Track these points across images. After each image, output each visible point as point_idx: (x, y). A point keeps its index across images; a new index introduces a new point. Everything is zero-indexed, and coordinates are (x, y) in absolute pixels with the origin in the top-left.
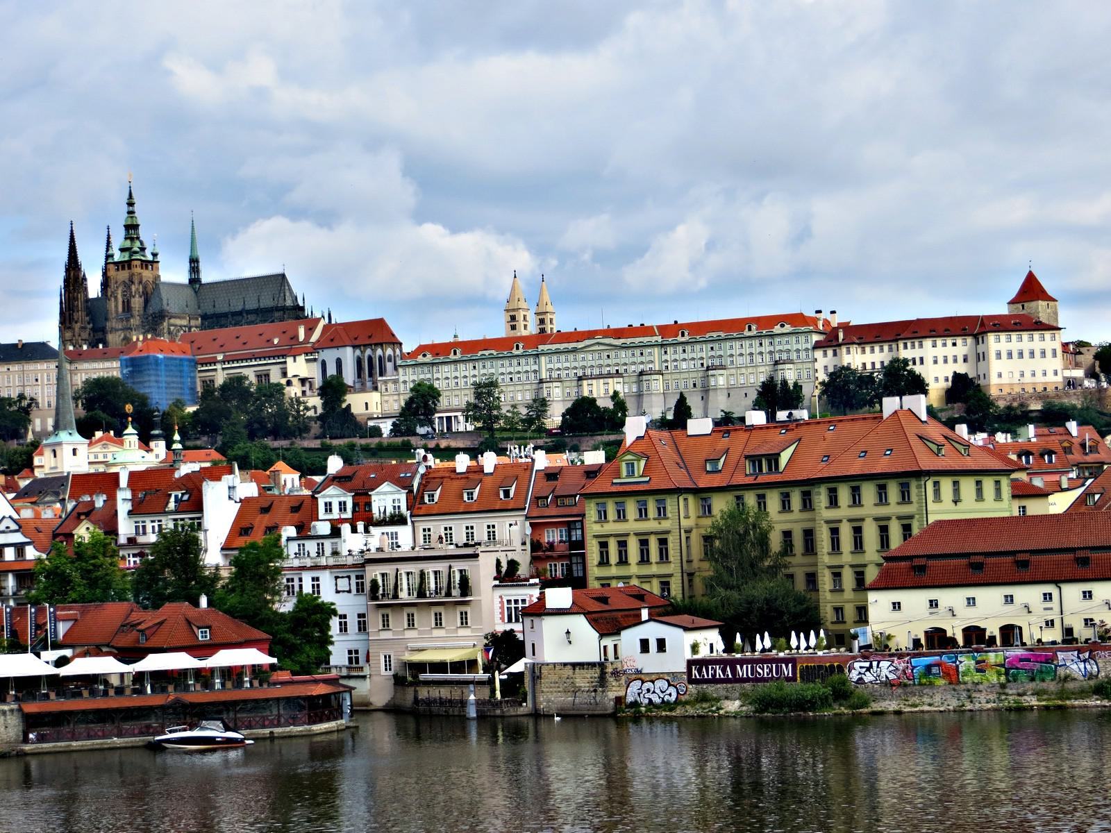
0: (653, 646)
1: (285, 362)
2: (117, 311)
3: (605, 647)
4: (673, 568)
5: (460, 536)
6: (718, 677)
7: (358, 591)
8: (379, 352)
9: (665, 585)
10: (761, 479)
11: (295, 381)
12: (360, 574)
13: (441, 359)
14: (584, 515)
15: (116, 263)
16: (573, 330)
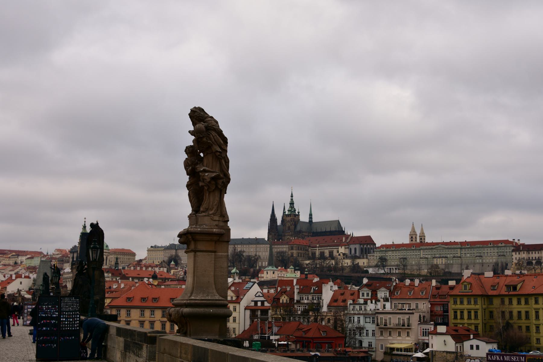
0: (475, 347)
1: (338, 248)
2: (286, 230)
3: (457, 347)
4: (479, 321)
6: (497, 359)
7: (373, 323)
8: (369, 246)
9: (476, 327)
10: (510, 293)
11: (341, 254)
12: (374, 317)
13: (388, 249)
14: (449, 302)
15: (286, 215)
16: (432, 242)
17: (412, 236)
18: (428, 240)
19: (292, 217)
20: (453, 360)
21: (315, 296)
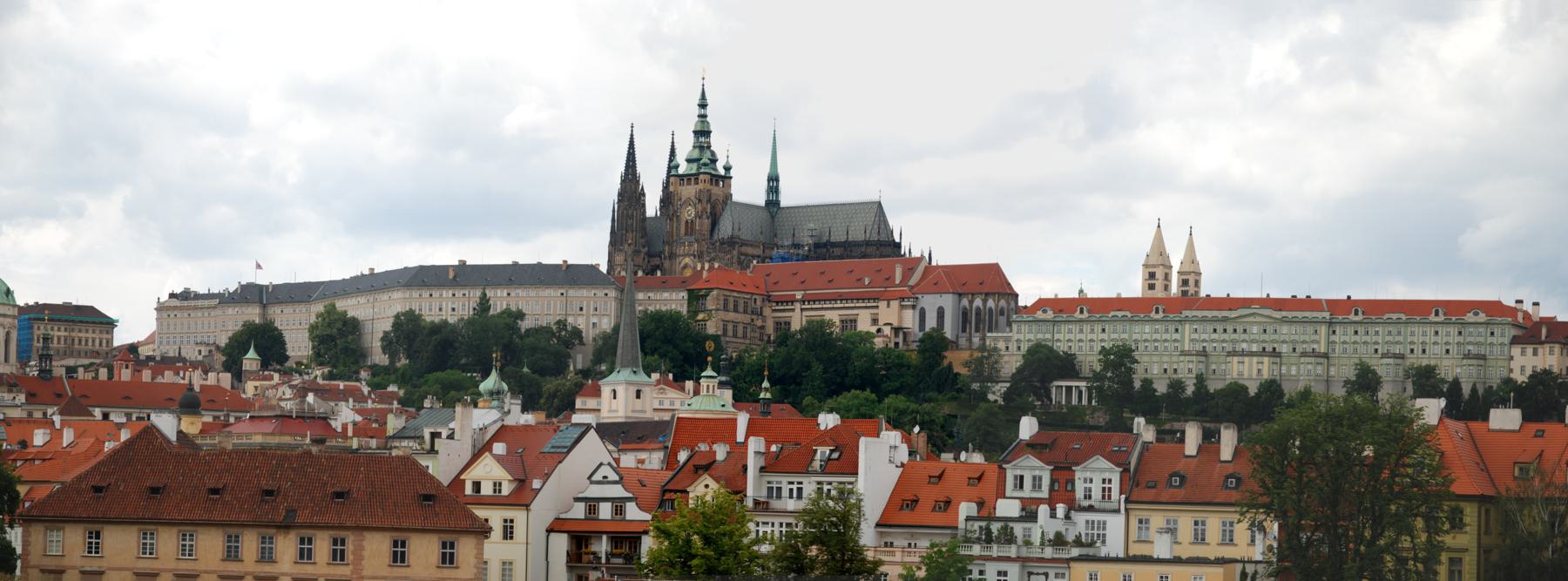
1: (877, 307)
2: (678, 235)
15: (681, 177)
16: (1225, 296)
17: (1152, 270)
18: (1210, 287)
19: (701, 186)
21: (830, 483)
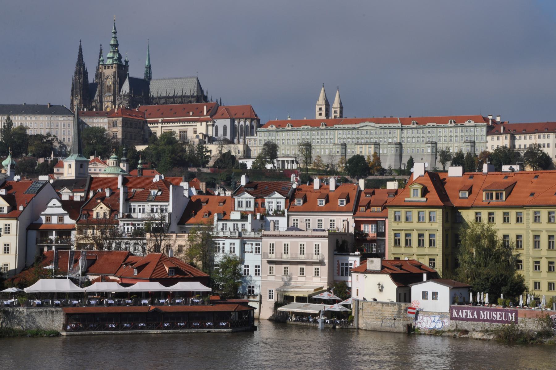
0: (430, 295)
1: (196, 125)
5: (314, 225)
6: (468, 317)
7: (256, 252)
9: (432, 261)
17: (320, 107)
20: (394, 317)
21: (157, 206)
